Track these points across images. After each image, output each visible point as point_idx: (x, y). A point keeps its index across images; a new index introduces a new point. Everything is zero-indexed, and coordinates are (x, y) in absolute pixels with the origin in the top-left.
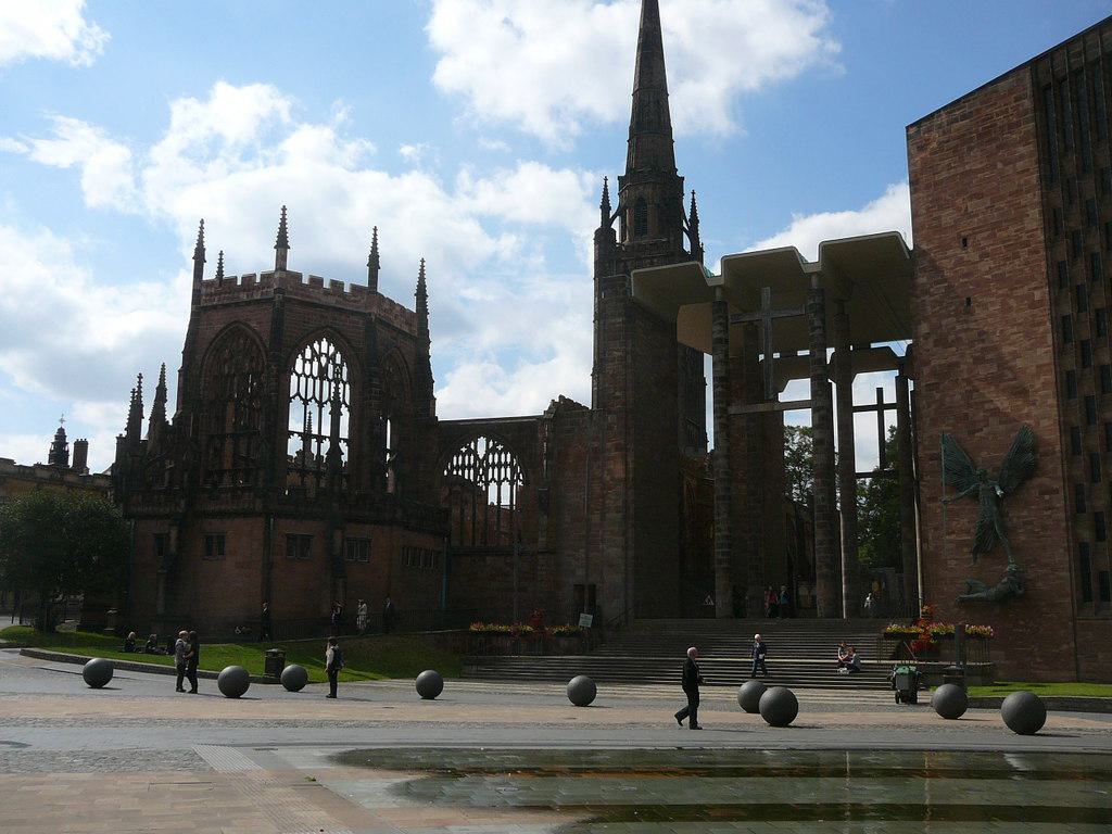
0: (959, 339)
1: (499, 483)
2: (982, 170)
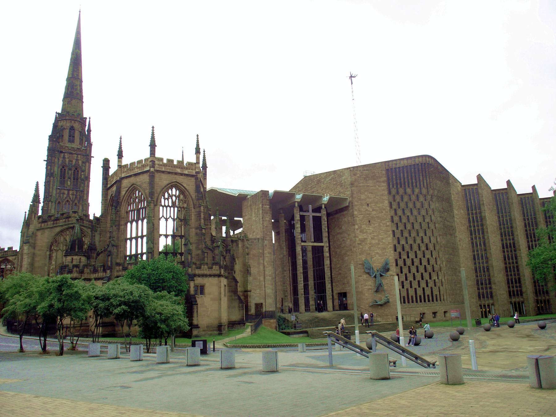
0: (367, 232)
2: (372, 186)
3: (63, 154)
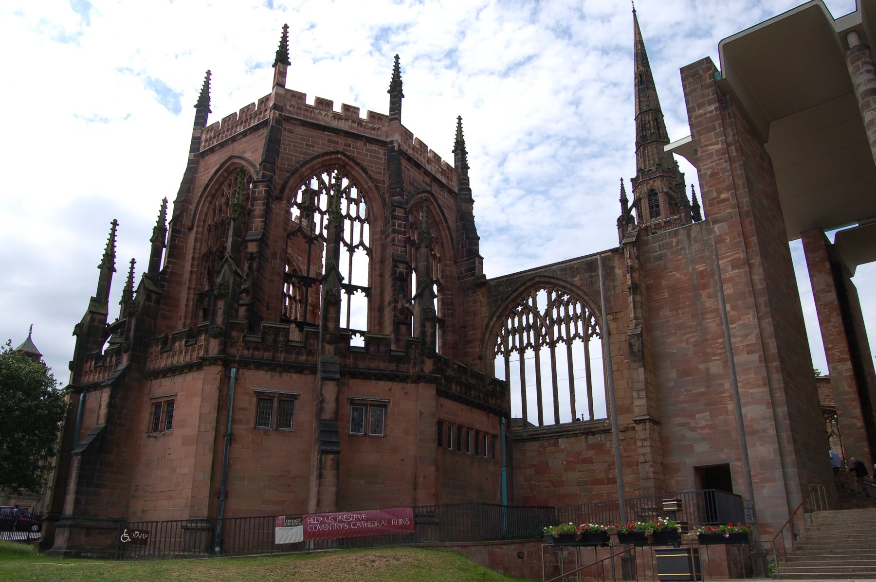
1: (569, 342)
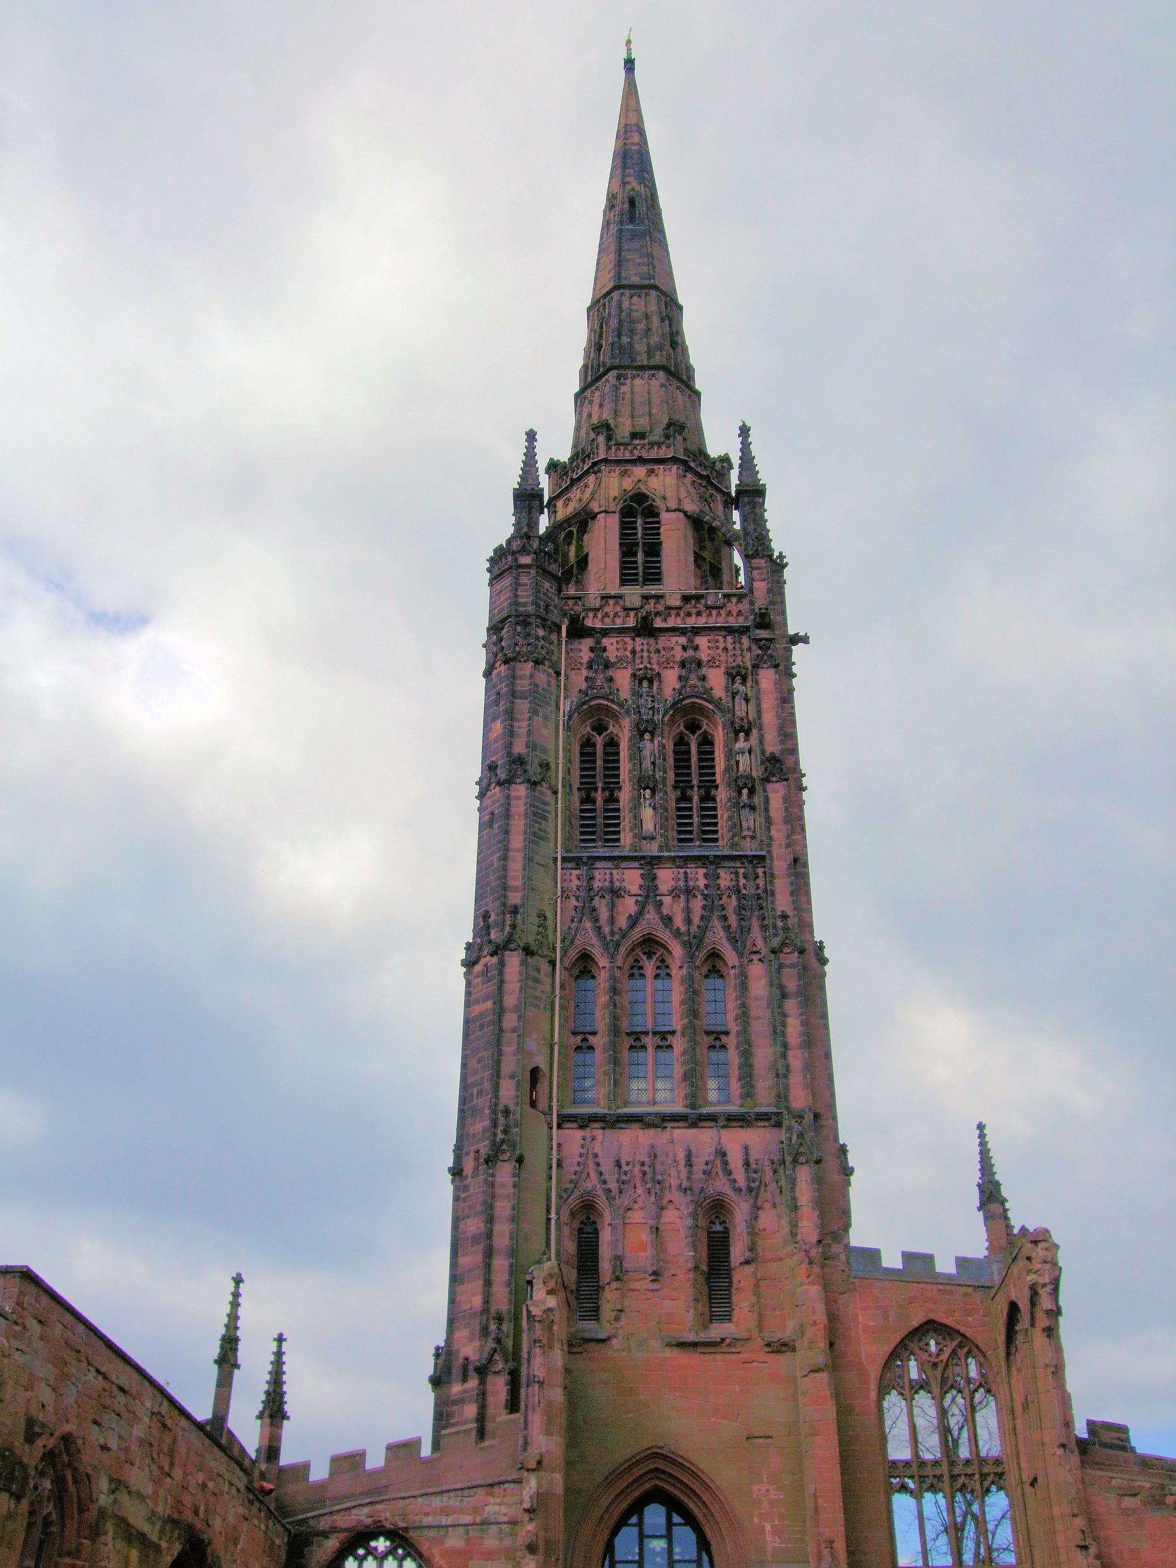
3: (588, 642)
